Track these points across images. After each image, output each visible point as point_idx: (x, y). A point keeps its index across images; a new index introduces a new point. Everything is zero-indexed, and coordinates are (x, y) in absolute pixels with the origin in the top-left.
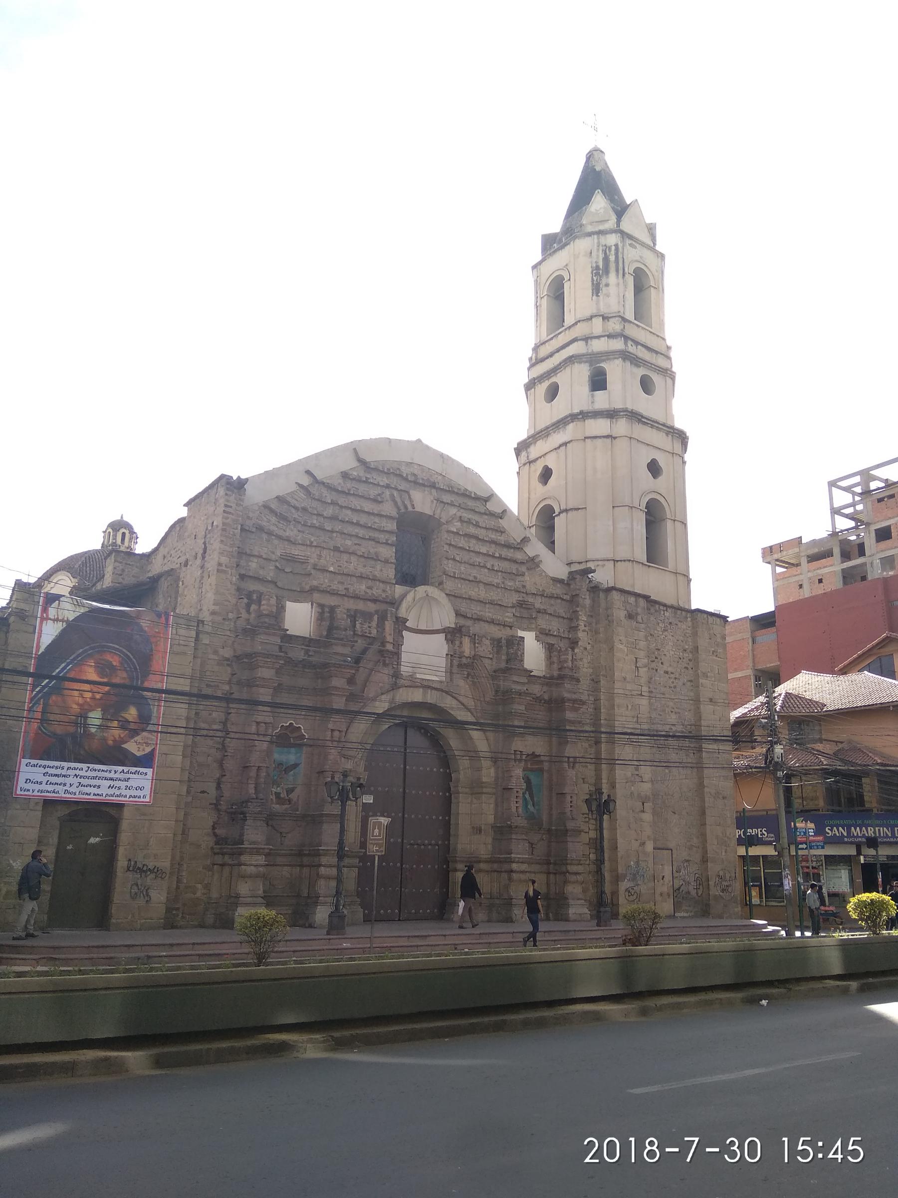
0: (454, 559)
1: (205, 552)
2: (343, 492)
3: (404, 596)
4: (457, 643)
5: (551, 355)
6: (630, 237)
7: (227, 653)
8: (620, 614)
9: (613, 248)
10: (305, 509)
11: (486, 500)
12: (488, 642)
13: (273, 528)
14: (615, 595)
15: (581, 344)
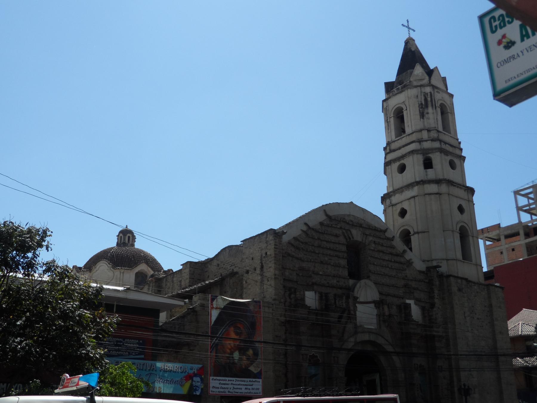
0: (374, 264)
1: (262, 267)
2: (322, 233)
3: (355, 285)
4: (381, 308)
5: (400, 148)
6: (437, 88)
7: (283, 319)
8: (455, 289)
9: (429, 94)
10: (306, 243)
11: (385, 231)
12: (395, 307)
13: (294, 254)
14: (452, 279)
15: (417, 144)
